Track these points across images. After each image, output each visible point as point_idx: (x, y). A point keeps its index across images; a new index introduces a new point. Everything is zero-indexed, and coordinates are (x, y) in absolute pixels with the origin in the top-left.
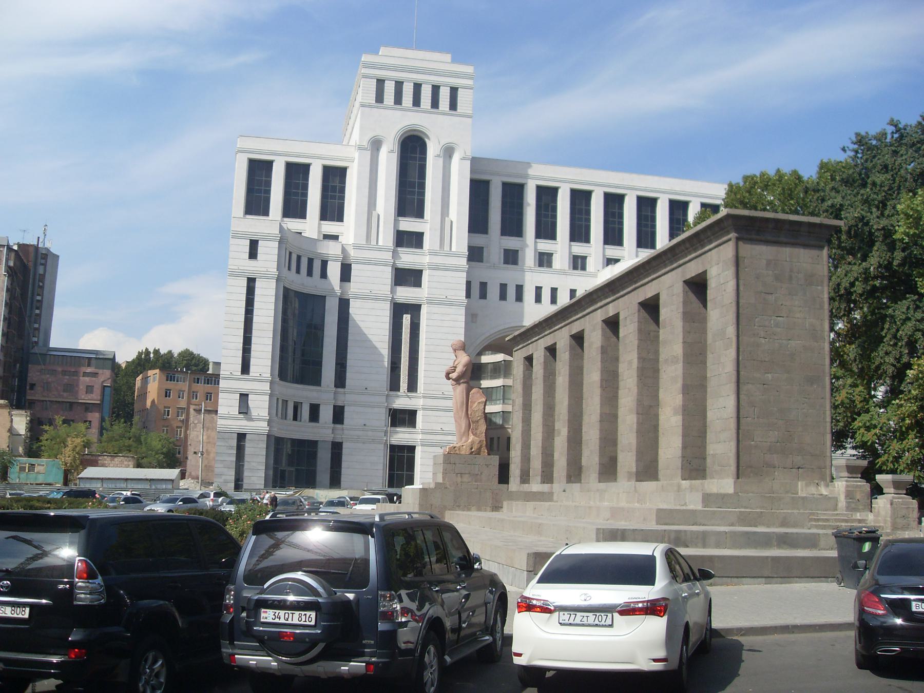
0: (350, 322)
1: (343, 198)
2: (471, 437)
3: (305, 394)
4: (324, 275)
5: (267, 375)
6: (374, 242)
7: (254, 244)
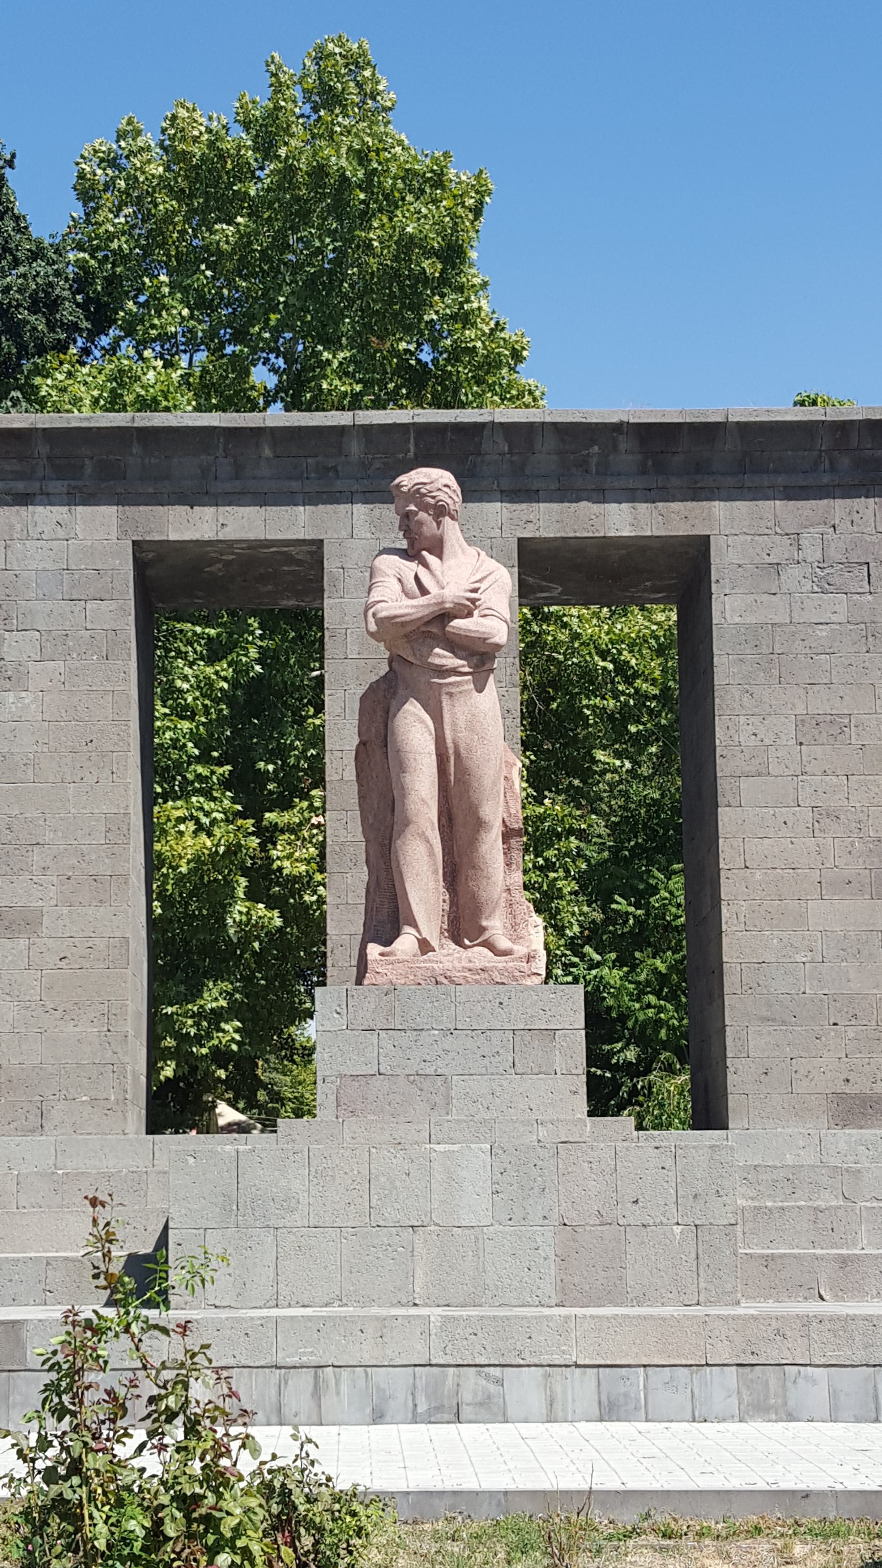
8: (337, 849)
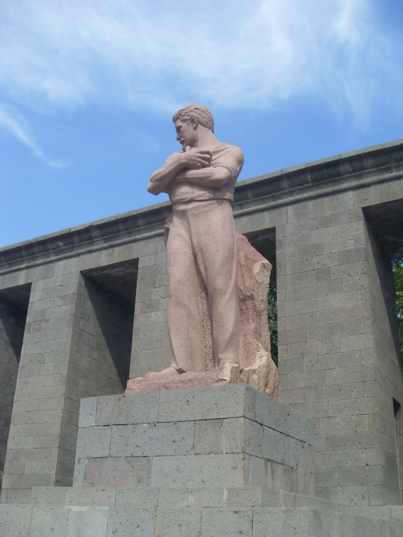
8: (283, 363)
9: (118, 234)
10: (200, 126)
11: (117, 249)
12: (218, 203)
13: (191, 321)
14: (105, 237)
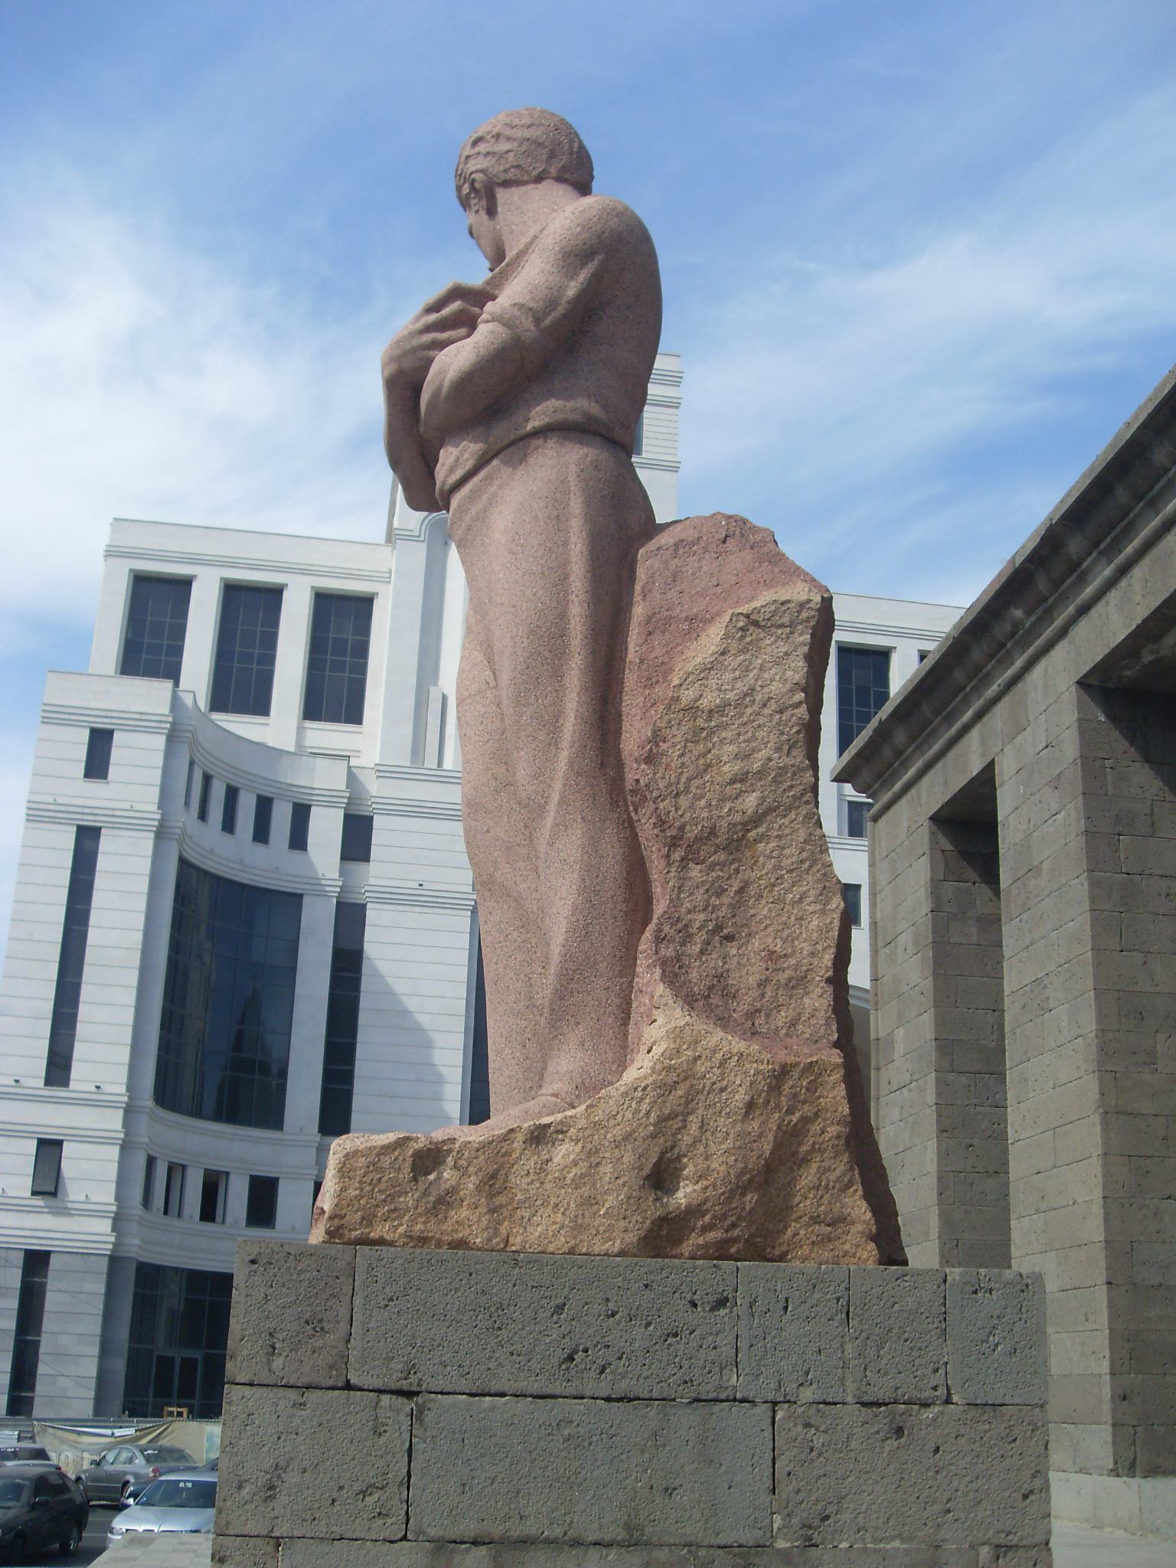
0: (365, 962)
1: (361, 669)
2: (662, 1026)
3: (238, 1150)
4: (299, 839)
5: (117, 1086)
6: (431, 762)
7: (100, 743)
9: (1126, 521)
10: (502, 195)
11: (1137, 573)
12: (506, 463)
13: (534, 941)
14: (1102, 546)
